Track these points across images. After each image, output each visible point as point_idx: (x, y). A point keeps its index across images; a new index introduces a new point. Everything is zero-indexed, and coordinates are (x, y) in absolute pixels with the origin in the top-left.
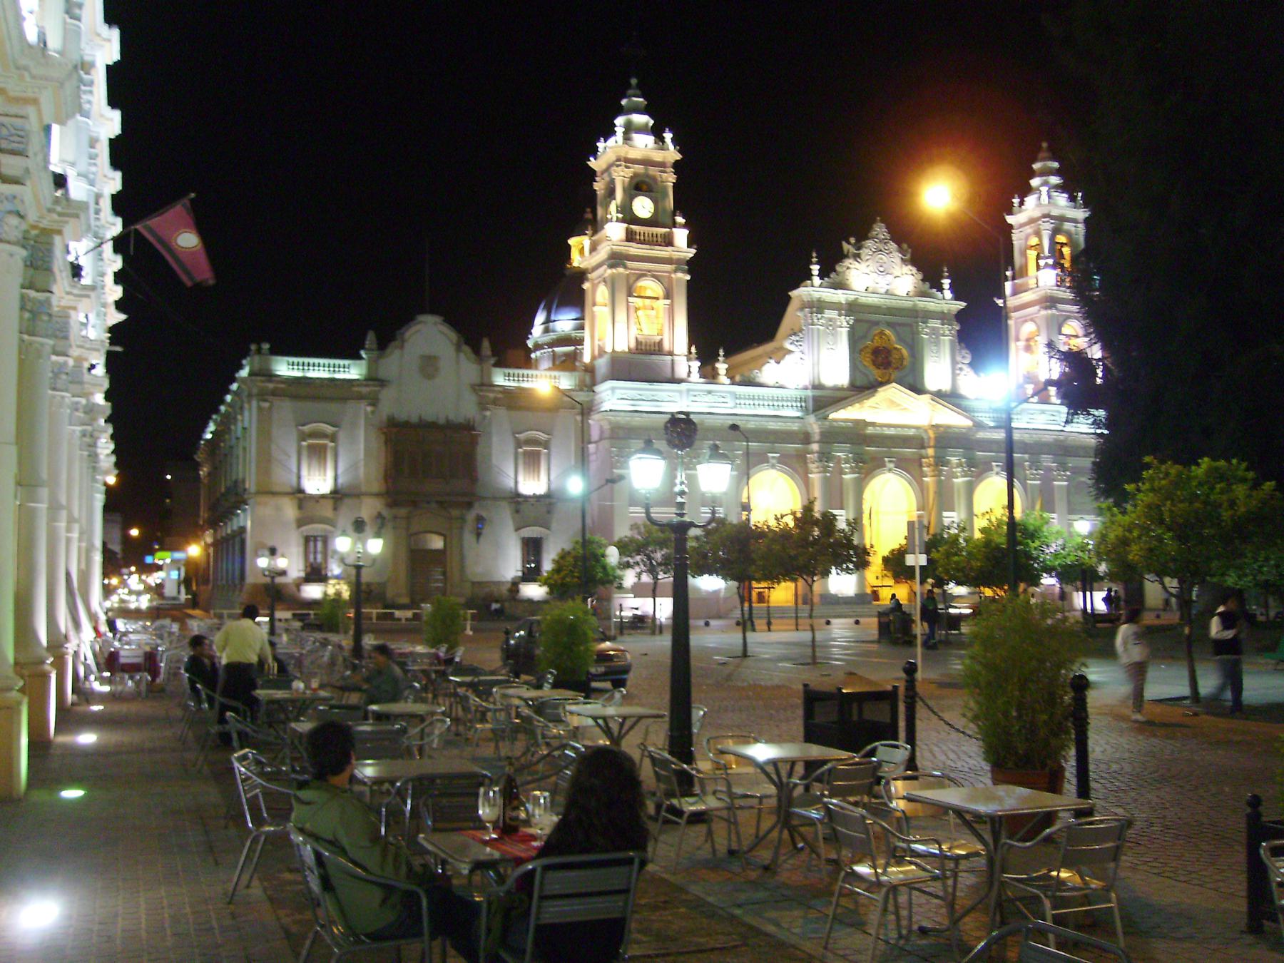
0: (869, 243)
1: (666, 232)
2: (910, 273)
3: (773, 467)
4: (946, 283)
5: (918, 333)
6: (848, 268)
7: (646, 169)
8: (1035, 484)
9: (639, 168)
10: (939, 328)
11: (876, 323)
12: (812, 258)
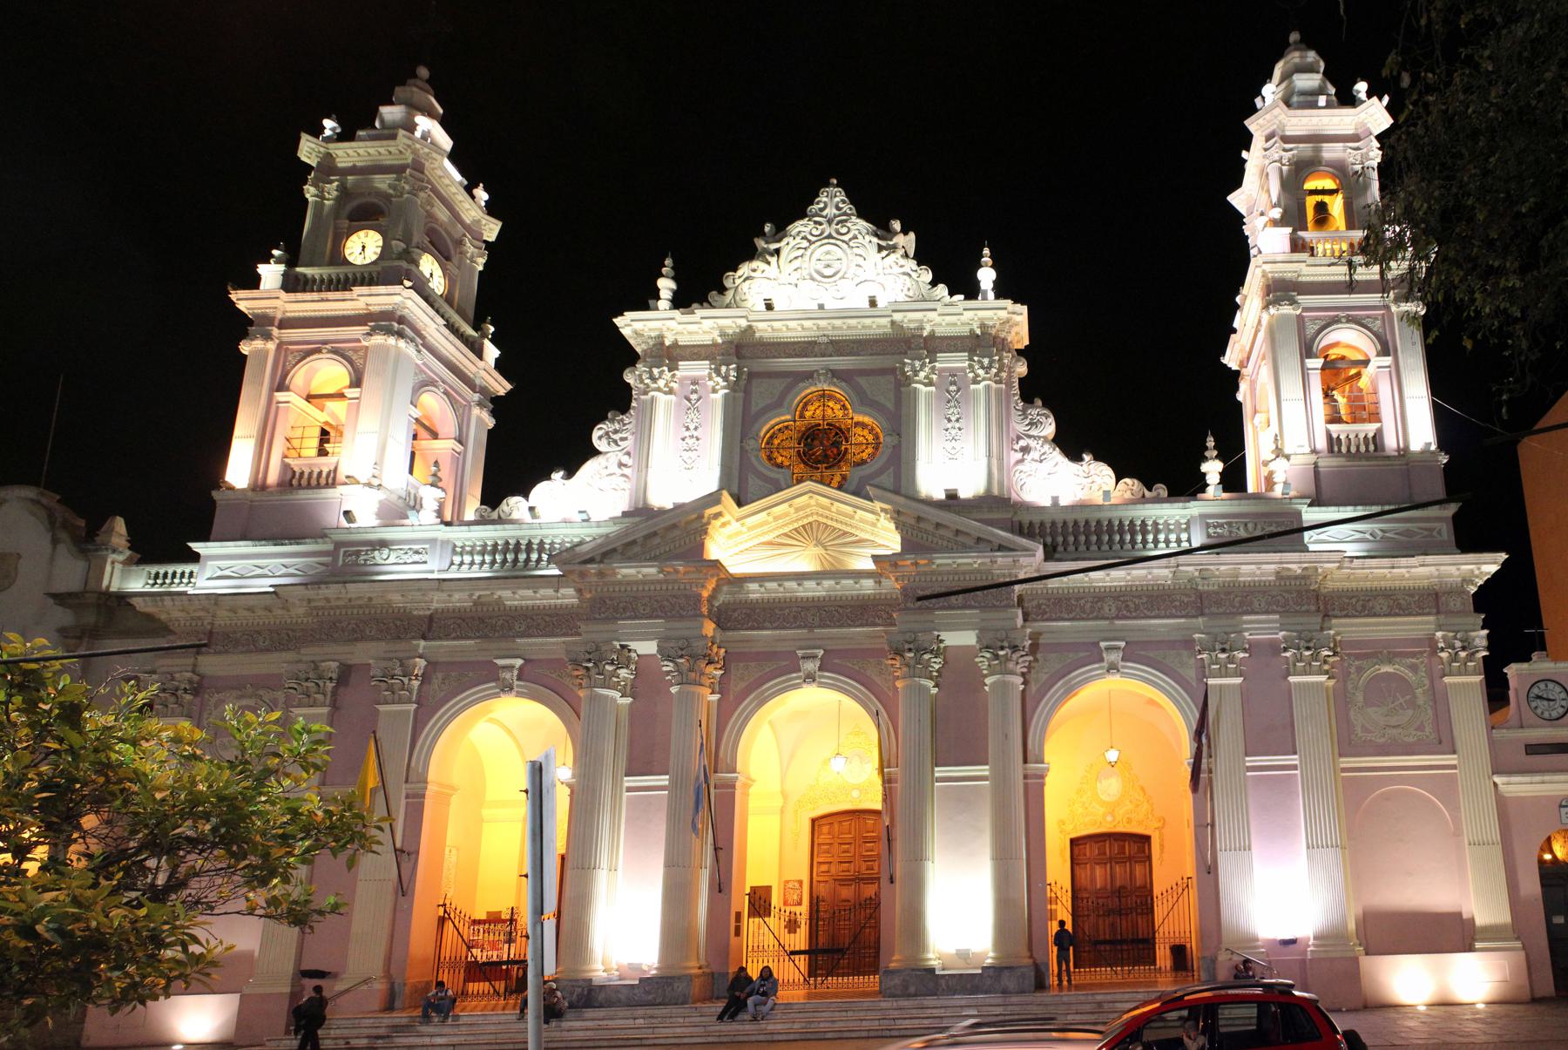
2: (897, 270)
5: (908, 381)
8: (1234, 685)
10: (963, 369)
11: (808, 376)
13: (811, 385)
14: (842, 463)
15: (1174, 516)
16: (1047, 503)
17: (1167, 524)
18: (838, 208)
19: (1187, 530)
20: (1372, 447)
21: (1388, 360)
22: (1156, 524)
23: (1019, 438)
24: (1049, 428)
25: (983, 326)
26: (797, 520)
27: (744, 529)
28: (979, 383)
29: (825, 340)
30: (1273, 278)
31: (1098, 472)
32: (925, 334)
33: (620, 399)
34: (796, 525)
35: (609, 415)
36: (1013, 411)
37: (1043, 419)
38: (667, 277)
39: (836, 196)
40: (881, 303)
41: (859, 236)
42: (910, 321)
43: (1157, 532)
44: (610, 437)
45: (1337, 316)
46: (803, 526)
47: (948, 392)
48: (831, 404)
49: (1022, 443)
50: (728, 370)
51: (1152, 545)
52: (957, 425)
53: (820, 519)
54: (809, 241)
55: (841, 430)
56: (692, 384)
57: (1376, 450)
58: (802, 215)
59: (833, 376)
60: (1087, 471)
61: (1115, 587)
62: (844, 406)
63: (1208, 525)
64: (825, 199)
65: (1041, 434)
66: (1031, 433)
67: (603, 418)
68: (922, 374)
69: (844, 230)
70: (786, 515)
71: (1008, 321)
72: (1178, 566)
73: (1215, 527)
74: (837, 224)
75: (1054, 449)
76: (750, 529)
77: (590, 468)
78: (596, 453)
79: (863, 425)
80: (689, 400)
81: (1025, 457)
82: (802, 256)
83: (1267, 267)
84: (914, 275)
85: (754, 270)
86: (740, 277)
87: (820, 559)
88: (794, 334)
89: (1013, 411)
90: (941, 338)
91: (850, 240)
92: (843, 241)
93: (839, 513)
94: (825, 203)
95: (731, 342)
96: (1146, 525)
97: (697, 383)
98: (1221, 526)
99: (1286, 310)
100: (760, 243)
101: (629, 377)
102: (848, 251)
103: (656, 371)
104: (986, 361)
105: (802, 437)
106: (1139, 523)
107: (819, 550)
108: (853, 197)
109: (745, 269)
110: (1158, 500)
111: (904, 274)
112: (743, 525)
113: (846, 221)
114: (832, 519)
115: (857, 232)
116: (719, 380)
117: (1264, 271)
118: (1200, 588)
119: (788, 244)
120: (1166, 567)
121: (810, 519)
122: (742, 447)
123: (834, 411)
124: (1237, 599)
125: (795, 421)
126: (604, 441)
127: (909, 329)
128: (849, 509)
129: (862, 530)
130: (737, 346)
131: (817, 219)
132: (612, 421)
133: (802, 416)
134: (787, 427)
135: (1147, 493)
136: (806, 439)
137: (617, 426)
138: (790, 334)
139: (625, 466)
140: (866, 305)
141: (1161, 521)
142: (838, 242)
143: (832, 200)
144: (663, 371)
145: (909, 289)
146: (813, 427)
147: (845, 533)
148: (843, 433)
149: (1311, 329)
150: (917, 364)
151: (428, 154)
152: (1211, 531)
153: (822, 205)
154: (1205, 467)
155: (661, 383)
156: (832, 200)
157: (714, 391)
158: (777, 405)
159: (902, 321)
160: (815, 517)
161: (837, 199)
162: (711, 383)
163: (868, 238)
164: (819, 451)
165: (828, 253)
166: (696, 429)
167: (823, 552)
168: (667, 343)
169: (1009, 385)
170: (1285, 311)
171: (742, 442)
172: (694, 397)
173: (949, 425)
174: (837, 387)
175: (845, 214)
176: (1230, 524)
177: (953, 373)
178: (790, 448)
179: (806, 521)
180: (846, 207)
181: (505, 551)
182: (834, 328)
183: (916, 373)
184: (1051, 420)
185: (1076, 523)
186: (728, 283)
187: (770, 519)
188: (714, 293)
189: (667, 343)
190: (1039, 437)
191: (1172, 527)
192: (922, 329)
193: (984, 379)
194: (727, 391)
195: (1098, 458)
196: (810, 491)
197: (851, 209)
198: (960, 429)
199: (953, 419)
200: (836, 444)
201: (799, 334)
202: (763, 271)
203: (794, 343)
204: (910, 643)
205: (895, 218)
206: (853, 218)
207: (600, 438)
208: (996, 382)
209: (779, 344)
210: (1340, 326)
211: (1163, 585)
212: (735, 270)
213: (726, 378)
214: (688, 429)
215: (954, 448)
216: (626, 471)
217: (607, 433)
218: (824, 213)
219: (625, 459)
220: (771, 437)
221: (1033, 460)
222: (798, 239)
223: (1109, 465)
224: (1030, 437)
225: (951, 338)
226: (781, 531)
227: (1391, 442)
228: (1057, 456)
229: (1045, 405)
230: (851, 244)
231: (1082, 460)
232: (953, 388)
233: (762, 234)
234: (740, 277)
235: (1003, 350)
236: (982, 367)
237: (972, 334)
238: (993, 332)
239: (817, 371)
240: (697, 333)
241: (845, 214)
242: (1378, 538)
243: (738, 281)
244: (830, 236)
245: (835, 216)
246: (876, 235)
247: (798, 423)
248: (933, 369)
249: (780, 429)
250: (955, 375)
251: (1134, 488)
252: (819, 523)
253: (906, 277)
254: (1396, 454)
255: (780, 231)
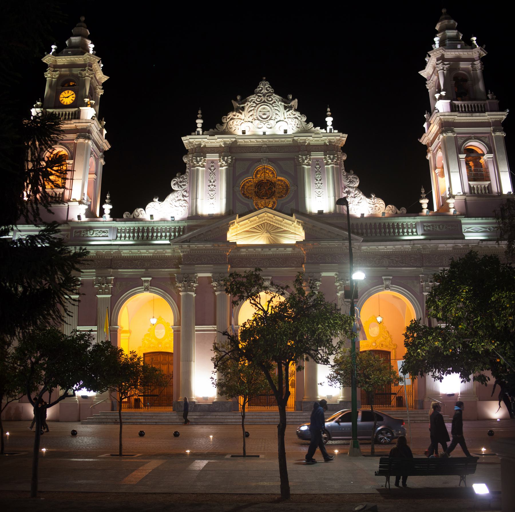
0: (253, 98)
1: (75, 112)
2: (292, 116)
3: (147, 289)
4: (329, 120)
5: (300, 164)
6: (232, 119)
7: (70, 71)
9: (66, 71)
10: (322, 159)
11: (259, 161)
12: (198, 114)
13: (260, 164)
14: (273, 197)
15: (410, 222)
16: (359, 216)
17: (407, 225)
18: (267, 90)
19: (415, 228)
20: (487, 191)
21: (491, 156)
22: (403, 225)
23: (345, 188)
24: (357, 184)
25: (330, 142)
26: (259, 222)
27: (239, 226)
28: (329, 165)
29: (266, 146)
30: (444, 121)
31: (378, 202)
32: (306, 144)
33: (182, 169)
34: (258, 224)
35: (177, 175)
36: (342, 176)
37: (355, 180)
38: (200, 119)
39: (266, 85)
40: (289, 133)
41: (276, 102)
42: (301, 140)
43: (403, 228)
44: (178, 184)
45: (470, 136)
46: (261, 224)
47: (316, 168)
48: (267, 171)
49: (347, 190)
50: (228, 159)
51: (401, 234)
52: (320, 182)
53: (268, 222)
54: (256, 103)
55: (272, 182)
56: (211, 163)
57: (489, 192)
58: (252, 93)
59: (269, 161)
60: (373, 201)
61: (388, 252)
62: (273, 172)
63: (424, 226)
64: (262, 86)
65: (354, 186)
66: (351, 185)
67: (175, 176)
68: (306, 161)
69: (270, 99)
70: (255, 220)
71: (340, 139)
72: (414, 244)
73: (427, 227)
74: (267, 97)
75: (360, 193)
76: (241, 226)
77: (171, 197)
78: (172, 191)
79: (281, 181)
80: (211, 170)
81: (348, 196)
82: (253, 110)
83: (442, 117)
84: (299, 118)
85: (234, 116)
86: (229, 118)
87: (268, 238)
88: (253, 143)
89: (342, 176)
90: (312, 145)
91: (273, 103)
92: (270, 104)
93: (276, 220)
94: (262, 87)
95: (228, 147)
96: (399, 225)
97: (214, 163)
98: (429, 226)
99: (450, 134)
100: (235, 104)
101: (185, 160)
102: (272, 108)
103: (198, 159)
104: (332, 156)
105: (256, 185)
106: (396, 224)
107: (268, 235)
108: (273, 85)
109: (231, 115)
110: (403, 215)
111: (296, 118)
112: (239, 225)
113: (271, 95)
114: (273, 222)
115: (275, 100)
116: (224, 162)
117: (440, 119)
118: (422, 252)
119: (247, 105)
120: (409, 245)
121: (264, 222)
122: (233, 190)
123: (270, 176)
124: (437, 257)
125: (253, 179)
126: (176, 186)
127: (300, 142)
128: (281, 219)
129: (285, 227)
130: (229, 148)
131: (259, 94)
132: (179, 177)
133: (256, 176)
134: (250, 181)
135: (398, 211)
136: (258, 186)
137: (181, 180)
138: (251, 143)
139: (185, 196)
140: (282, 133)
141: (405, 224)
142: (268, 104)
143: (264, 87)
144: (202, 159)
145: (298, 124)
146: (260, 181)
147: (278, 227)
148: (273, 184)
149: (460, 142)
150: (304, 157)
151: (94, 60)
152: (425, 228)
153: (261, 89)
154: (422, 201)
155: (200, 163)
156: (264, 87)
157: (221, 166)
158: (246, 172)
159: (298, 140)
160: (266, 221)
161: (267, 86)
162: (220, 163)
163: (280, 103)
164: (263, 191)
165: (264, 108)
166: (214, 182)
167: (269, 235)
168: (202, 146)
169: (340, 165)
170: (450, 135)
171: (233, 188)
172: (212, 168)
173: (317, 182)
174: (271, 165)
175: (270, 92)
176: (433, 225)
177: (317, 160)
178: (252, 190)
179: (262, 222)
180: (271, 90)
181: (138, 232)
182: (269, 141)
183: (303, 161)
184: (358, 180)
185: (371, 224)
186: (224, 121)
187: (249, 222)
188: (218, 124)
189: (202, 146)
190: (354, 187)
191: (409, 226)
192: (305, 142)
193: (331, 164)
194: (227, 167)
195: (377, 196)
196: (266, 212)
197: (272, 90)
198: (321, 184)
199: (318, 179)
200: (270, 188)
201: (255, 144)
202: (238, 116)
203: (253, 147)
204: (311, 277)
205: (290, 94)
206: (274, 94)
207: (174, 184)
208: (335, 165)
209: (246, 147)
210: (472, 140)
211: (408, 251)
212: (227, 115)
213: (226, 162)
214: (211, 182)
215: (319, 192)
216: (185, 198)
217: (177, 182)
218: (262, 92)
219: (185, 194)
220: (244, 185)
221: (351, 197)
222: (252, 103)
223: (382, 199)
224: (350, 187)
225: (316, 145)
226: (252, 226)
227: (495, 189)
228: (361, 196)
229: (355, 173)
230: (273, 105)
231: (371, 197)
232: (318, 166)
233: (236, 100)
234: (229, 118)
235: (338, 151)
236: (330, 159)
237: (325, 145)
238: (334, 144)
239: (262, 158)
240: (214, 142)
241: (270, 92)
242: (492, 231)
243: (228, 120)
244: (264, 102)
245: (267, 93)
246: (283, 101)
247: (254, 180)
248: (310, 159)
249: (247, 182)
250: (319, 161)
251: (393, 209)
252: (267, 223)
253: (296, 119)
254: (497, 194)
255: (244, 100)
